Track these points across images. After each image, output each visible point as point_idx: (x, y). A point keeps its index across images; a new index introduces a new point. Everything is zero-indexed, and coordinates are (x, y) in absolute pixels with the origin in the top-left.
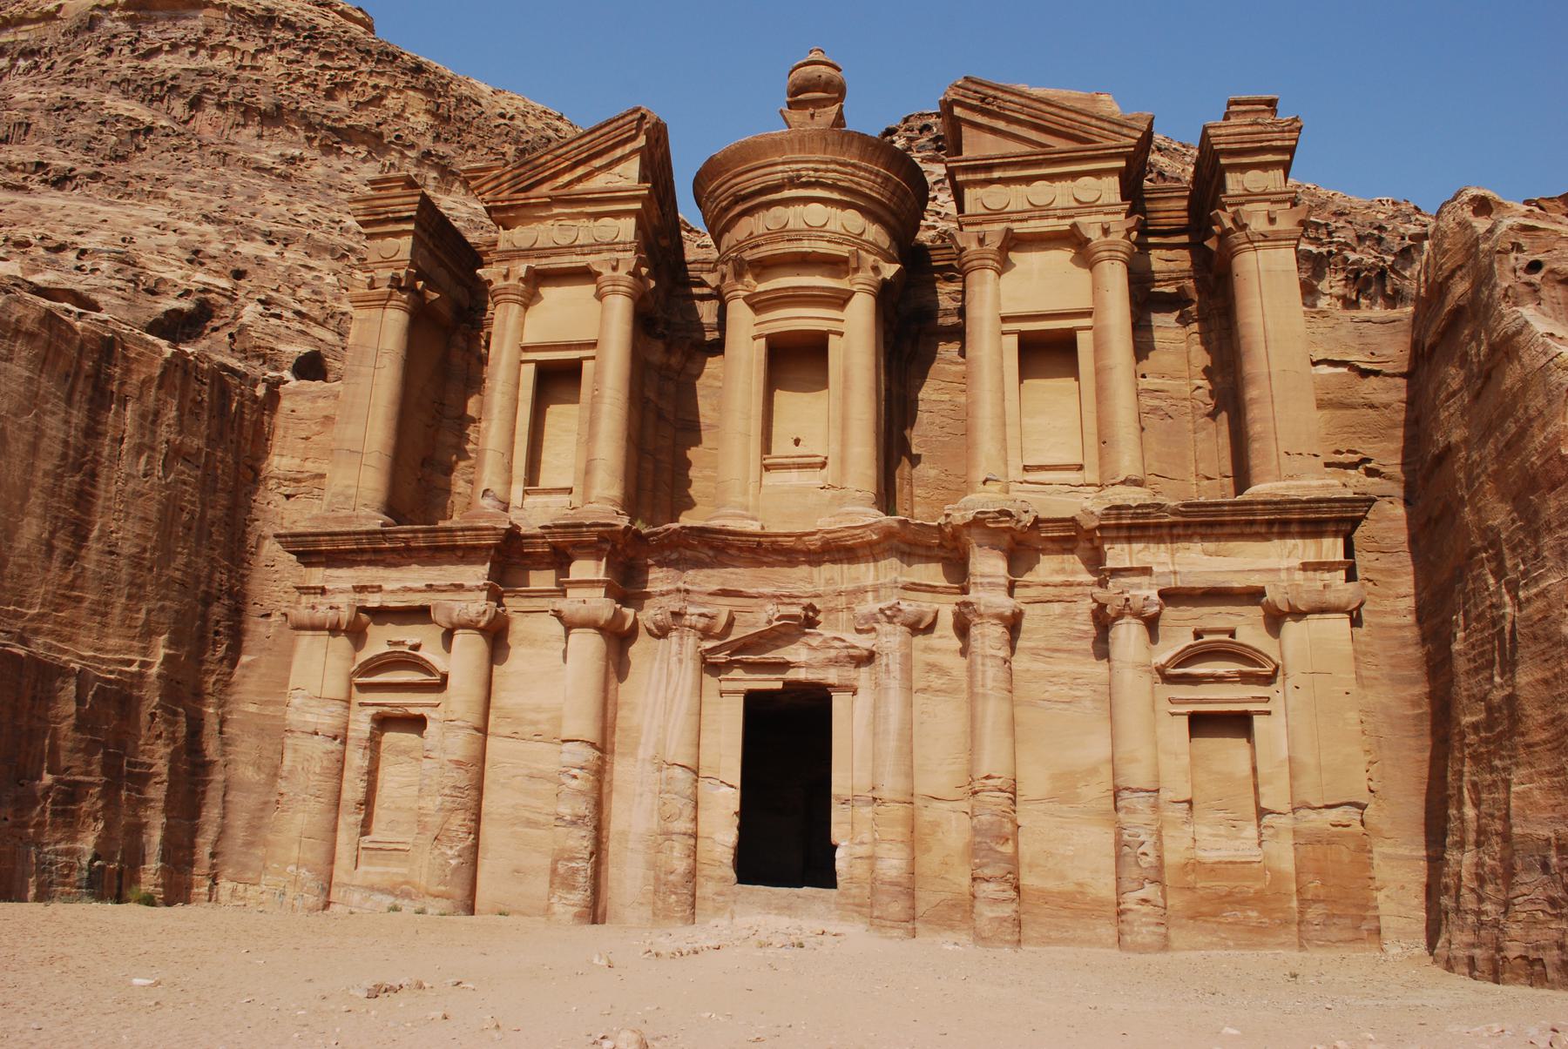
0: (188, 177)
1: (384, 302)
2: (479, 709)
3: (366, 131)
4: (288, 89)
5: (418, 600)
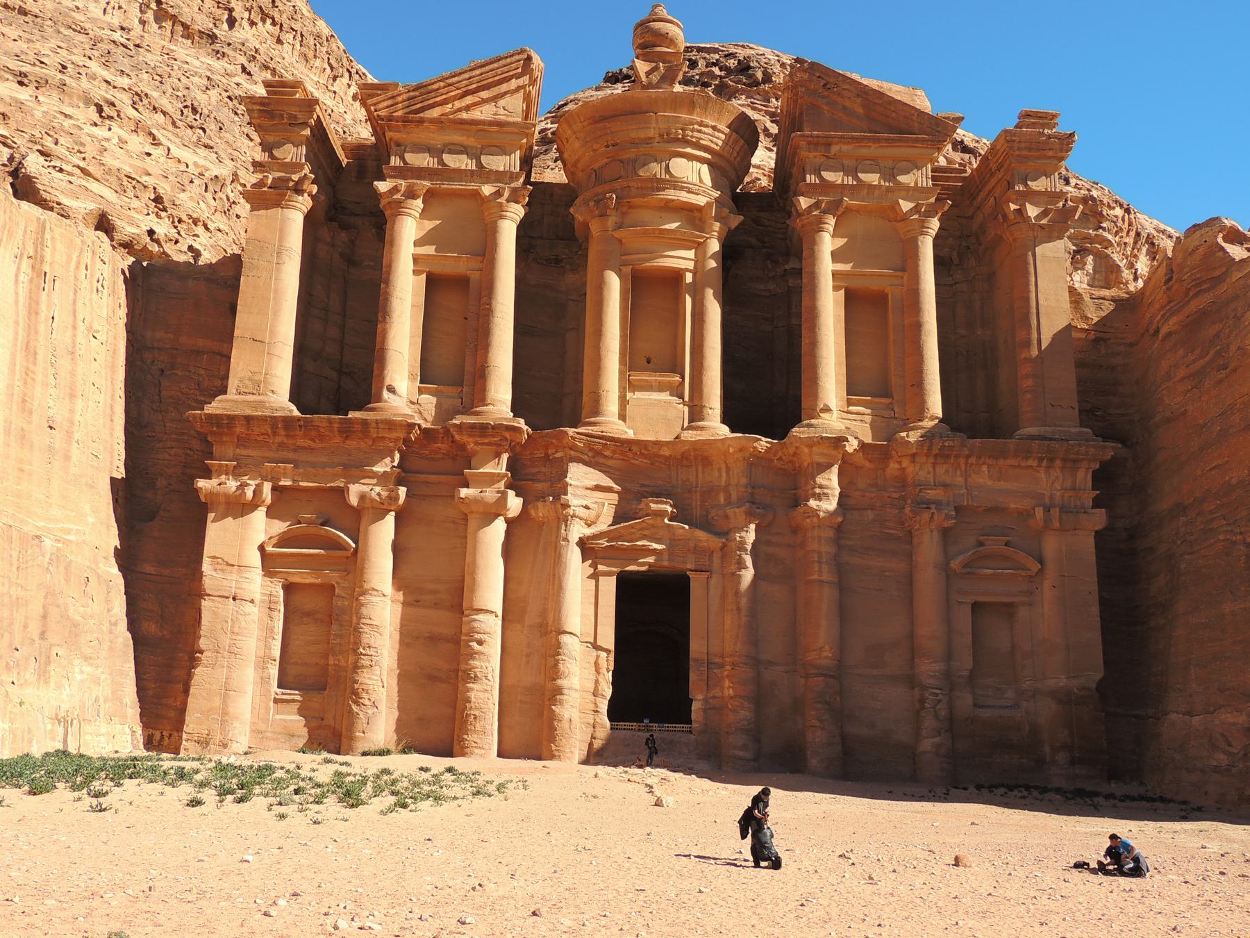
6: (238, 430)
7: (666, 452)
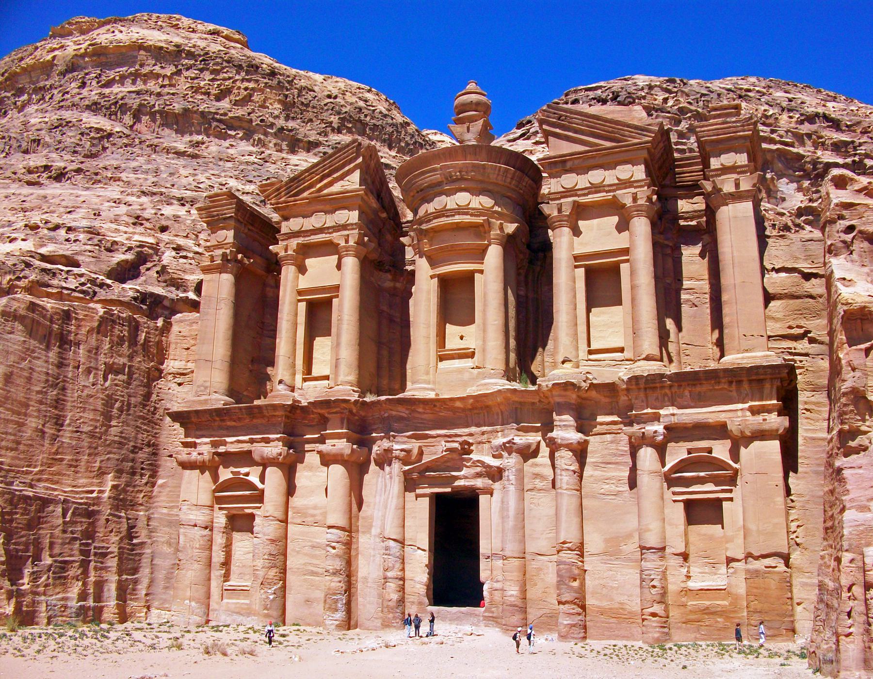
0: (134, 164)
1: (221, 269)
2: (282, 509)
4: (191, 97)
5: (246, 447)
6: (194, 419)
7: (458, 404)
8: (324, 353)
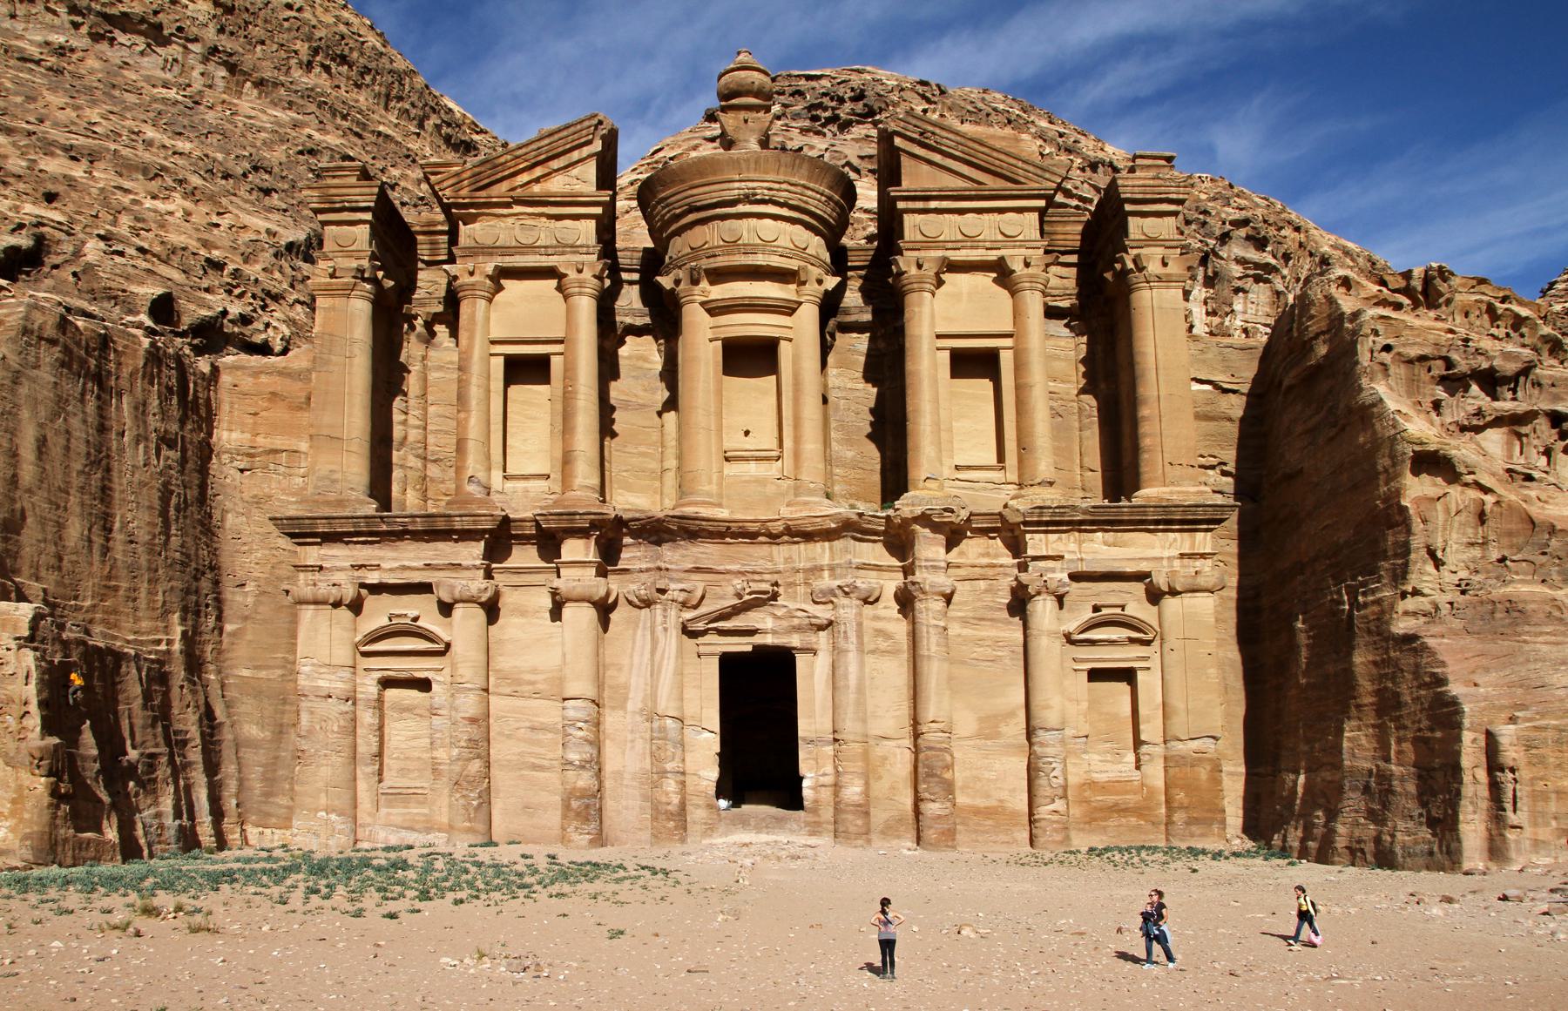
3: (143, 20)
8: (525, 440)
